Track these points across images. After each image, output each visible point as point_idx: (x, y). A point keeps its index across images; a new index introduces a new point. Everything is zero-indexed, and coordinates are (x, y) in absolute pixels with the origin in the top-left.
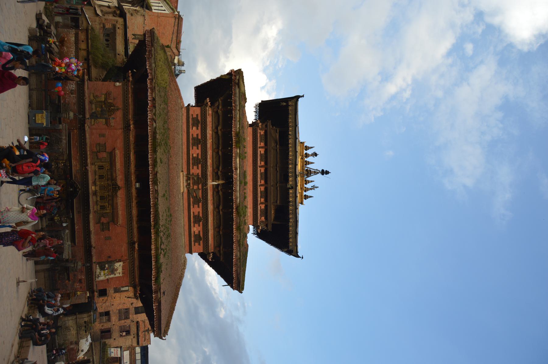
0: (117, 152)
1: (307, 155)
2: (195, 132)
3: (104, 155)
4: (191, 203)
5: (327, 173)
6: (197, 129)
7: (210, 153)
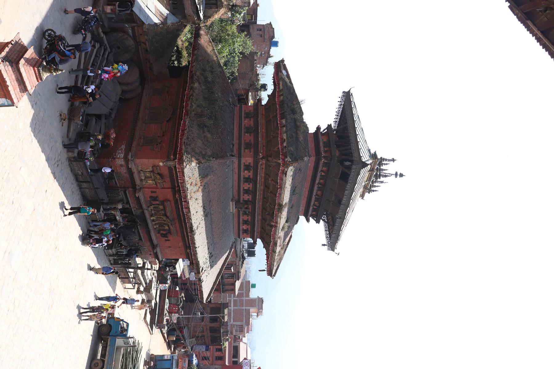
0: (167, 204)
1: (380, 164)
2: (246, 174)
3: (157, 202)
4: (241, 214)
5: (401, 175)
6: (249, 172)
7: (260, 187)
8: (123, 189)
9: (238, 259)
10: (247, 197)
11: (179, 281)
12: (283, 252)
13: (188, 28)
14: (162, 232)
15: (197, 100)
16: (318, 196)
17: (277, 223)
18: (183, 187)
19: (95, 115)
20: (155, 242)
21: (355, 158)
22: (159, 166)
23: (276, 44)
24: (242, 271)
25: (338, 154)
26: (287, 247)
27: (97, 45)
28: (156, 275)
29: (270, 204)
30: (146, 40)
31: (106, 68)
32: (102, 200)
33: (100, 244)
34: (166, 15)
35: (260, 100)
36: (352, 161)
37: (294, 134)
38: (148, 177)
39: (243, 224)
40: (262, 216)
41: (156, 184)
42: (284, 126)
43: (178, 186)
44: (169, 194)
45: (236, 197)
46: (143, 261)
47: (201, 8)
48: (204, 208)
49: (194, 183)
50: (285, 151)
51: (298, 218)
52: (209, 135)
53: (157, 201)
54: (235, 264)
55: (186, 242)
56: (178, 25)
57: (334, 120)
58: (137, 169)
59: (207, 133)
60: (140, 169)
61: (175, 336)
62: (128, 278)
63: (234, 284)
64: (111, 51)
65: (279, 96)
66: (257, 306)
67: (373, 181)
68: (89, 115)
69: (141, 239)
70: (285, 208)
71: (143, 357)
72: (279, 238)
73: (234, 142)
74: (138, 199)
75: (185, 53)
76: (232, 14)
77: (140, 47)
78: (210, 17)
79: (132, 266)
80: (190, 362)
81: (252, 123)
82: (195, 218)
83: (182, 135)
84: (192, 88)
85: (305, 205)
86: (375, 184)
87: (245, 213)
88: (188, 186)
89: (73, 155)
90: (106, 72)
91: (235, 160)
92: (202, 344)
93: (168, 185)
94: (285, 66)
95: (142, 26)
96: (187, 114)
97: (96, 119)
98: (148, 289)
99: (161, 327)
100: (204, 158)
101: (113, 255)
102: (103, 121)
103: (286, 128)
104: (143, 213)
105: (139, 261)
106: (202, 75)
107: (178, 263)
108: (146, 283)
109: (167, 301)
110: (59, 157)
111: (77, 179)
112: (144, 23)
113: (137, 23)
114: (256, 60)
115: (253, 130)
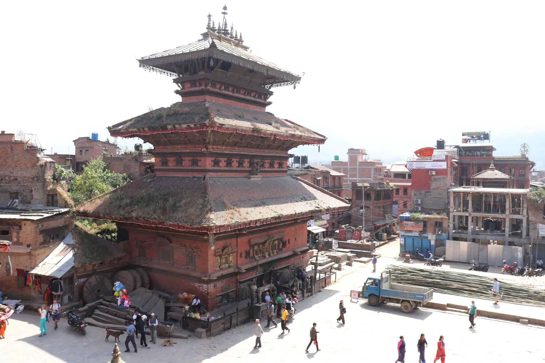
0: (253, 242)
1: (213, 30)
2: (223, 164)
3: (251, 251)
4: (263, 169)
5: (225, 8)
6: (221, 161)
7: (236, 151)
8: (238, 285)
9: (309, 173)
10: (246, 163)
11: (330, 229)
12: (301, 129)
13: (78, 223)
14: (281, 247)
15: (149, 214)
16: (245, 93)
17: (271, 134)
18: (234, 227)
19: (166, 313)
20: (290, 253)
21: (206, 55)
22: (215, 250)
23: (95, 136)
24: (321, 168)
25: (202, 73)
26: (296, 124)
27: (97, 312)
28: (323, 252)
29: (253, 141)
30: (90, 264)
31: (119, 303)
32: (248, 304)
33: (292, 305)
34: (65, 245)
35: (149, 151)
36: (210, 58)
37: (183, 117)
38: (227, 260)
39: (273, 167)
40: (265, 149)
41: (233, 253)
42: (174, 127)
43: (235, 231)
44: (243, 240)
45: (246, 174)
46: (309, 264)
47: (57, 210)
48: (256, 206)
49: (231, 216)
50: (199, 126)
51: (268, 113)
52: (184, 201)
53: (249, 251)
54: (314, 175)
55: (291, 224)
56: (75, 233)
57: (169, 76)
58: (218, 271)
59: (181, 203)
60: (218, 269)
61: (383, 234)
62: (325, 279)
63: (334, 177)
64: (103, 298)
65: (144, 131)
66: (356, 154)
67: (231, 37)
68: (166, 319)
69: (288, 267)
70: (256, 126)
71: (401, 264)
72: (287, 132)
73: (191, 176)
74: (248, 270)
75: (104, 226)
76: (64, 179)
77: (97, 271)
78: (66, 202)
79: (313, 275)
80: (408, 219)
81: (172, 159)
82: (266, 214)
83: (184, 228)
84: (137, 218)
85: (255, 106)
86: (234, 36)
87: (262, 166)
88: (234, 221)
89: (205, 332)
90: (122, 302)
91: (208, 175)
92: (391, 208)
93: (234, 240)
94: (114, 126)
95: (76, 268)
96: (162, 223)
97: (170, 311)
98: (337, 260)
99: (374, 247)
100: (206, 207)
101: (303, 293)
102: (171, 304)
103: (176, 124)
104: (261, 265)
105: (309, 268)
106: (124, 209)
107: (313, 231)
108: (331, 262)
109: (349, 241)
110: (206, 346)
111: (229, 329)
112: (73, 267)
113: (73, 274)
114: (111, 156)
115: (179, 157)
